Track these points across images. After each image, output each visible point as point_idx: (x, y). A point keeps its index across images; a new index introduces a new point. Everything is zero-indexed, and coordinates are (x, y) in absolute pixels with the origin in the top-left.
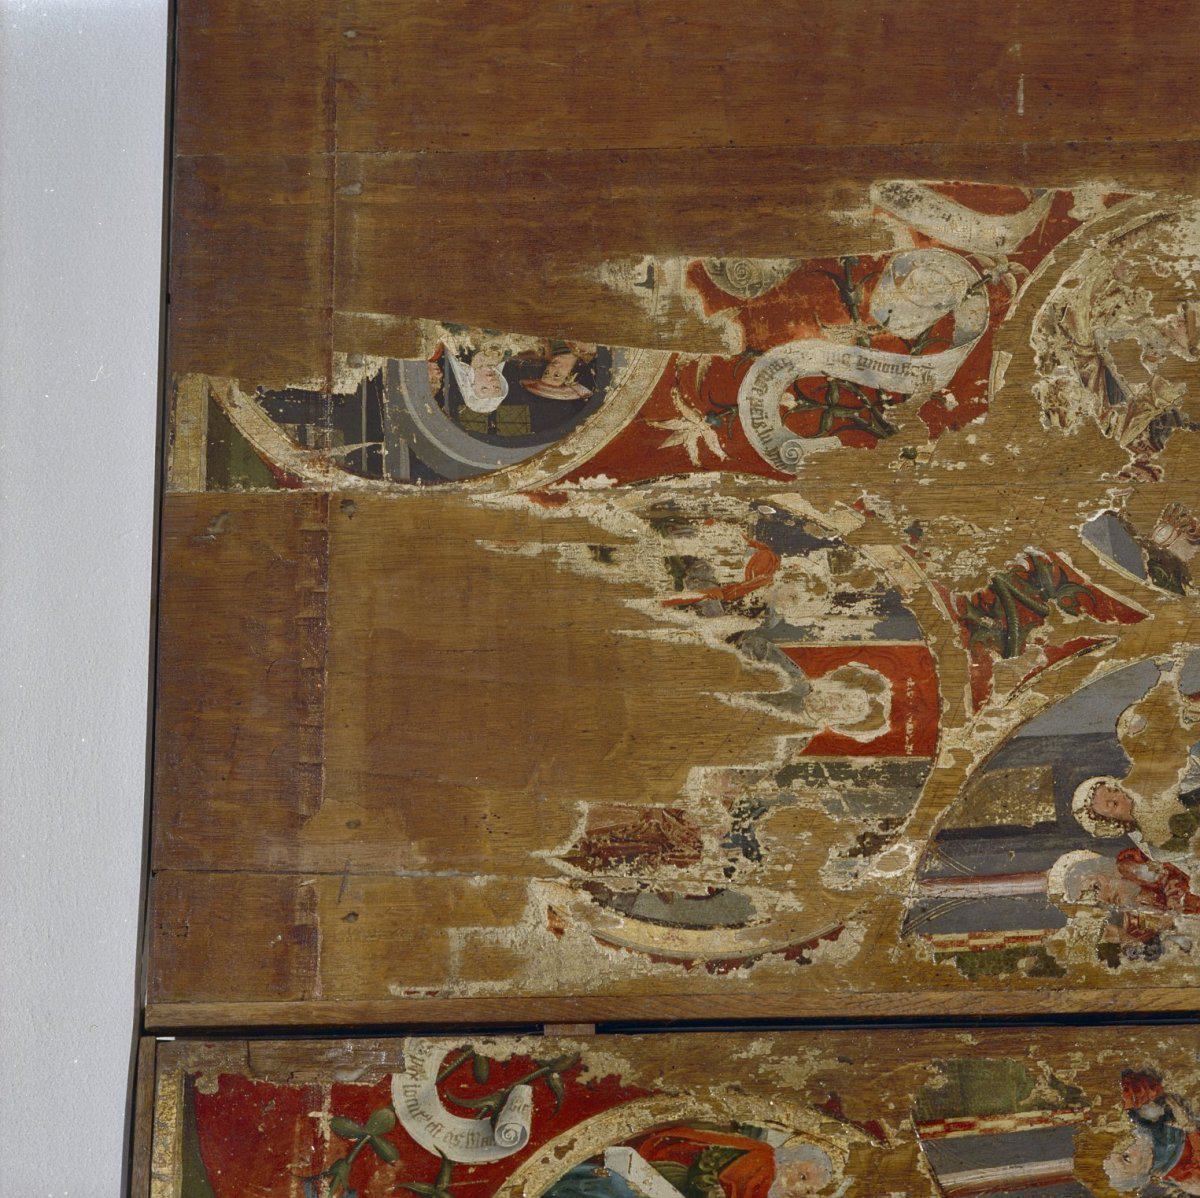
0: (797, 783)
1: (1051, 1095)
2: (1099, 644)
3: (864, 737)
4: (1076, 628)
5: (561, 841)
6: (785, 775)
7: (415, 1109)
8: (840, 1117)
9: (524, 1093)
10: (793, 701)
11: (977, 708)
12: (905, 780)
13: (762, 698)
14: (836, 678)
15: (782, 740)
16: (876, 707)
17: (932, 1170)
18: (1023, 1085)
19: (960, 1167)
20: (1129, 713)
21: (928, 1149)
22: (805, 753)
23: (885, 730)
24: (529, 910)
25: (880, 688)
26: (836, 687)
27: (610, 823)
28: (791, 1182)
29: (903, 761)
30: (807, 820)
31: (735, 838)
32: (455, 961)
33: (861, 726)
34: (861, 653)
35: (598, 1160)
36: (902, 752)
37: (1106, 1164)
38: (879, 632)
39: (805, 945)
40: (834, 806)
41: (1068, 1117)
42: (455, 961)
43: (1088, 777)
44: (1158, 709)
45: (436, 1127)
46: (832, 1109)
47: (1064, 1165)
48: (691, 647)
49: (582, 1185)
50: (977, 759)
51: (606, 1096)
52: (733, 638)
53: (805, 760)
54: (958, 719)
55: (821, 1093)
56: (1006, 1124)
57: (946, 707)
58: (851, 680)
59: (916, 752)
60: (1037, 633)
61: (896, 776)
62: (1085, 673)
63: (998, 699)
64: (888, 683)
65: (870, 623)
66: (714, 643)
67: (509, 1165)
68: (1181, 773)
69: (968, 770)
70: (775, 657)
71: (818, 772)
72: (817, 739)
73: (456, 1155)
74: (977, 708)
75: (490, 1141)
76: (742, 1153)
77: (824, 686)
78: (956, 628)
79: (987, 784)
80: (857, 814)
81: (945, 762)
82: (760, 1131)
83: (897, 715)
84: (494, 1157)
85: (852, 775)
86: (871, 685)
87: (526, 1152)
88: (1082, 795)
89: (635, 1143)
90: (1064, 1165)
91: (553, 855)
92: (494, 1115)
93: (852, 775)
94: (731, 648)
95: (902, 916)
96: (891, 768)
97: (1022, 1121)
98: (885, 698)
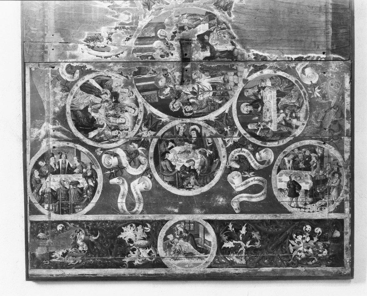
0: (118, 29)
1: (152, 72)
2: (162, 8)
3: (128, 22)
4: (159, 6)
5: (83, 38)
6: (116, 28)
7: (63, 73)
8: (122, 75)
9: (78, 71)
10: (117, 16)
11: (144, 18)
12: (133, 29)
13: (113, 16)
14: (124, 13)
15: (115, 23)
16: (130, 18)
17: (135, 83)
18: (148, 71)
19: (139, 82)
20: (166, 19)
21: (134, 80)
22: (119, 25)
23: (131, 21)
24: (78, 49)
25: (130, 15)
26: (124, 14)
27: (90, 35)
28: (115, 84)
29: (133, 26)
30: (118, 35)
31: (108, 38)
32: (68, 56)
33: (128, 20)
34: (127, 9)
35: (88, 81)
36: (133, 25)
37: (159, 82)
38: (130, 6)
39: (118, 55)
40: (123, 33)
41: (154, 75)
42: (68, 56)
43: (160, 29)
44: (171, 18)
45: (65, 76)
46: (121, 74)
47: (153, 82)
48: (102, 8)
49: (86, 85)
50: (144, 26)
51: (90, 72)
52: (109, 7)
53: (119, 26)
54: (141, 20)
55: (120, 71)
56: (145, 76)
57: (140, 18)
58: (126, 13)
59: (135, 25)
60: (153, 6)
61: (132, 29)
62: (160, 13)
63: (147, 16)
64: (131, 14)
65: (129, 4)
66: (106, 7)
67: (76, 82)
68: (173, 29)
69: (143, 28)
70: (115, 9)
71: (121, 28)
72: (121, 23)
73: (68, 80)
74: (144, 18)
75: (73, 78)
76: (108, 80)
77: (122, 14)
78: (142, 5)
79: (145, 30)
80: (126, 34)
81: (139, 26)
82: (111, 77)
83: (133, 19)
84: (74, 80)
85: (126, 28)
86: (129, 14)
87: (78, 80)
88: (159, 32)
89: (93, 78)
90: (153, 82)
91: (82, 40)
92: (74, 74)
93: (126, 28)
94: (108, 8)
95: (132, 50)
96: (131, 27)
97: (148, 76)
98: (131, 16)
